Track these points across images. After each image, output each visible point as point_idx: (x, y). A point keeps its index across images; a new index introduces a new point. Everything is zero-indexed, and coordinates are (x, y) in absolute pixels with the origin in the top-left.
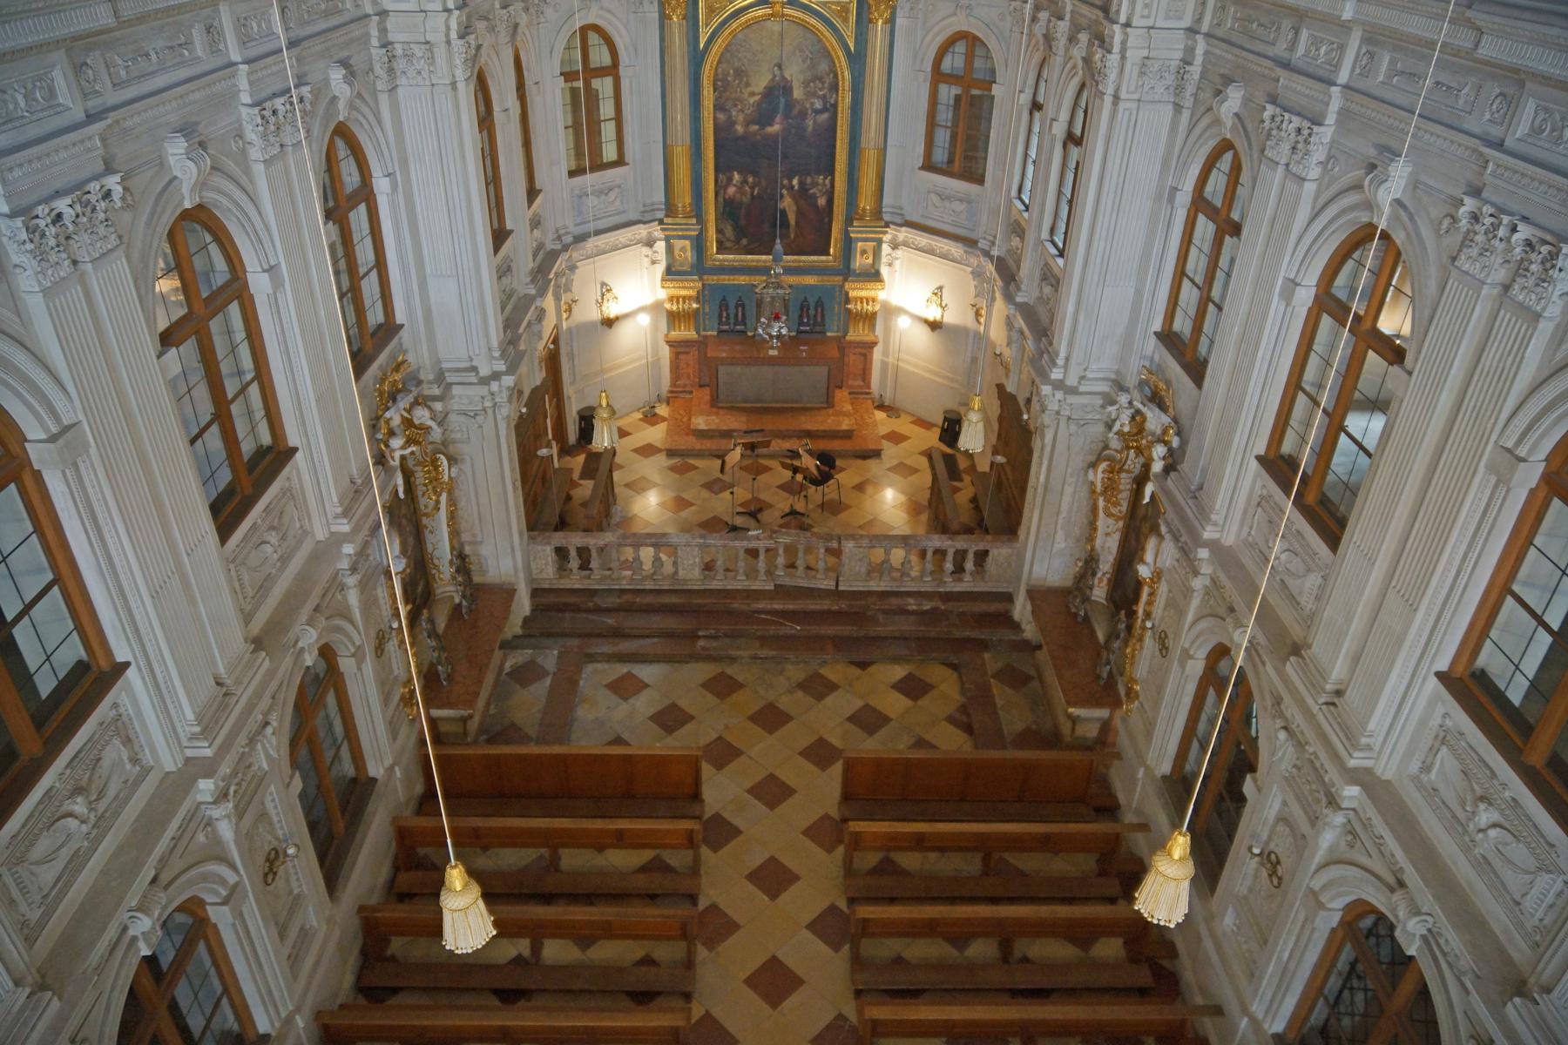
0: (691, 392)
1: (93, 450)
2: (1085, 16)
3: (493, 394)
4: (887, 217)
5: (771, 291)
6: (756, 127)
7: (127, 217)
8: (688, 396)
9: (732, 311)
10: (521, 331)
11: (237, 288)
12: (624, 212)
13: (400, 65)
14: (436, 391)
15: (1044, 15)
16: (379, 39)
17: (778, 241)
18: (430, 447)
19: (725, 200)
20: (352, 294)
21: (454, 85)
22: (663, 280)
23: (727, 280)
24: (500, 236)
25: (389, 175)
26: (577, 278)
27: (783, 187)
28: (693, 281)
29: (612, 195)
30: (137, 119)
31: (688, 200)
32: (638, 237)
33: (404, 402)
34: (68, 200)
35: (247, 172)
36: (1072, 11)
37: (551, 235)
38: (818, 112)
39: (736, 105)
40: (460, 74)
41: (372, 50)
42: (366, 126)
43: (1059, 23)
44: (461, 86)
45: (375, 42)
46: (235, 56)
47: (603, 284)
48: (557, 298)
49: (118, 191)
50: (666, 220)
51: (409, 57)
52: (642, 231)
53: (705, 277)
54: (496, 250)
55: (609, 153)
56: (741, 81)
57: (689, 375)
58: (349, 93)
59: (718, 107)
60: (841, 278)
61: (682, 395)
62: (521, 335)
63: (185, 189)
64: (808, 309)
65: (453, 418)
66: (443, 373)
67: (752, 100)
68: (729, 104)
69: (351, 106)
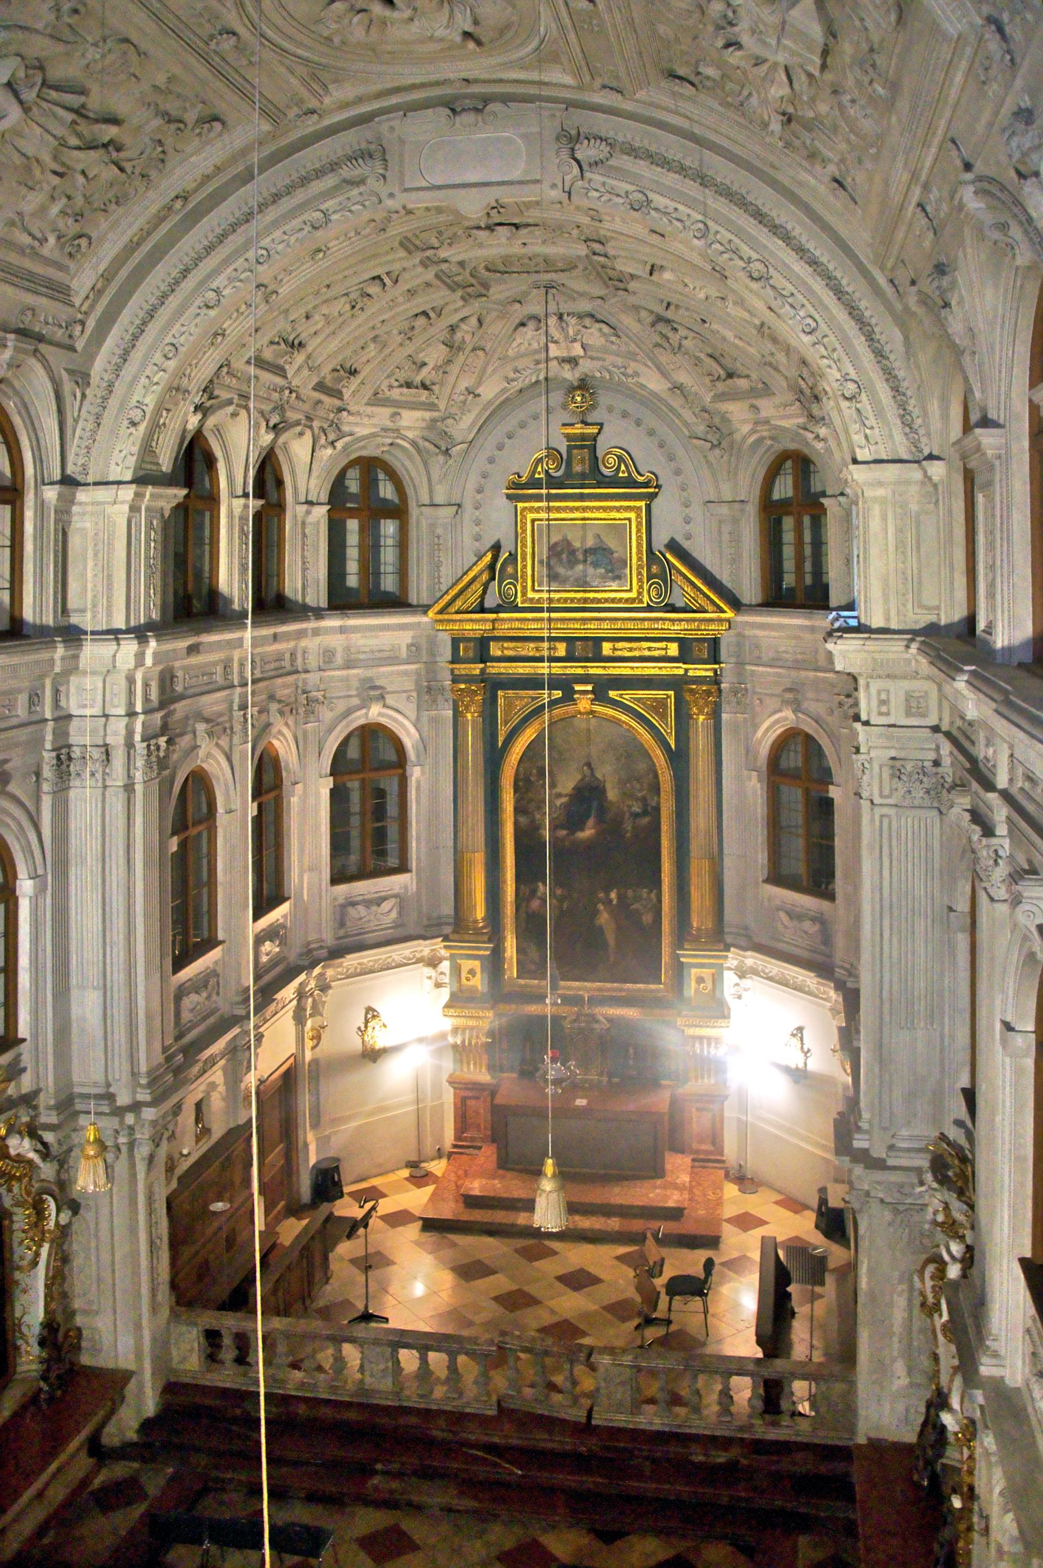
0: (480, 1148)
4: (729, 939)
6: (564, 832)
8: (476, 1152)
12: (402, 925)
16: (53, 742)
18: (37, 1185)
21: (129, 788)
27: (600, 901)
29: (386, 906)
32: (418, 955)
38: (636, 815)
40: (139, 776)
41: (45, 754)
44: (139, 788)
45: (48, 746)
47: (369, 1009)
52: (424, 948)
59: (518, 810)
61: (467, 1151)
68: (532, 806)
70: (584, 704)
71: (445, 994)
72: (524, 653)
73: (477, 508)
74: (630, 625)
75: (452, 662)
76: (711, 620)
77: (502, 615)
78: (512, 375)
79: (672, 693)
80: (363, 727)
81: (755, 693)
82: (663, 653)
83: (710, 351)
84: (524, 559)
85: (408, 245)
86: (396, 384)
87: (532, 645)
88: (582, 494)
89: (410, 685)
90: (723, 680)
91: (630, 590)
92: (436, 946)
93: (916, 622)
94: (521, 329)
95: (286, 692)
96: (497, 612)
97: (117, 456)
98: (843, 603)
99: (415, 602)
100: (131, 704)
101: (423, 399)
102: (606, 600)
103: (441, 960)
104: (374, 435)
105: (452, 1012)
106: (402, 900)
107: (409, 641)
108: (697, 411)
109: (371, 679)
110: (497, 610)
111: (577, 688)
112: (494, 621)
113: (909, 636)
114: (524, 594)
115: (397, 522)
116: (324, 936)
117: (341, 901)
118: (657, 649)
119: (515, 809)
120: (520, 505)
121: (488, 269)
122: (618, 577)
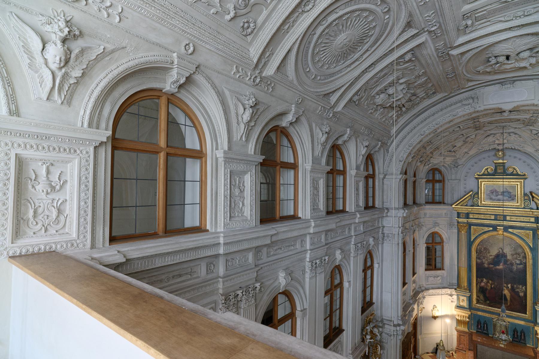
1: (307, 316)
3: (397, 331)
5: (500, 322)
6: (493, 266)
7: (326, 265)
9: (482, 325)
10: (407, 313)
11: (341, 285)
13: (386, 238)
14: (381, 325)
17: (503, 305)
19: (480, 286)
20: (364, 291)
21: (398, 244)
22: (455, 308)
23: (480, 313)
24: (404, 284)
25: (378, 263)
26: (425, 300)
28: (467, 311)
29: (439, 278)
30: (333, 245)
31: (466, 284)
32: (447, 293)
33: (372, 325)
34: (319, 260)
35: (349, 259)
37: (418, 287)
38: (518, 264)
39: (484, 258)
42: (375, 251)
45: (380, 233)
46: (353, 234)
48: (418, 306)
49: (327, 260)
50: (457, 289)
51: (388, 237)
52: (449, 291)
53: (472, 311)
54: (403, 287)
55: (439, 265)
56: (486, 252)
57: (464, 344)
58: (373, 244)
60: (533, 324)
62: (407, 315)
63: (338, 261)
64: (517, 332)
65: (383, 334)
66: (383, 320)
67: (491, 257)
68: (482, 258)
69: (373, 246)
70: (501, 232)
71: (455, 304)
72: (480, 217)
73: (465, 181)
80: (433, 232)
82: (529, 220)
87: (483, 215)
88: (487, 178)
91: (517, 203)
92: (453, 292)
99: (447, 203)
100: (399, 225)
101: (453, 154)
102: (509, 205)
103: (453, 295)
104: (439, 163)
105: (458, 310)
106: (443, 278)
107: (445, 212)
109: (436, 221)
111: (498, 228)
116: (423, 284)
117: (427, 275)
119: (476, 258)
120: (480, 180)
122: (513, 200)
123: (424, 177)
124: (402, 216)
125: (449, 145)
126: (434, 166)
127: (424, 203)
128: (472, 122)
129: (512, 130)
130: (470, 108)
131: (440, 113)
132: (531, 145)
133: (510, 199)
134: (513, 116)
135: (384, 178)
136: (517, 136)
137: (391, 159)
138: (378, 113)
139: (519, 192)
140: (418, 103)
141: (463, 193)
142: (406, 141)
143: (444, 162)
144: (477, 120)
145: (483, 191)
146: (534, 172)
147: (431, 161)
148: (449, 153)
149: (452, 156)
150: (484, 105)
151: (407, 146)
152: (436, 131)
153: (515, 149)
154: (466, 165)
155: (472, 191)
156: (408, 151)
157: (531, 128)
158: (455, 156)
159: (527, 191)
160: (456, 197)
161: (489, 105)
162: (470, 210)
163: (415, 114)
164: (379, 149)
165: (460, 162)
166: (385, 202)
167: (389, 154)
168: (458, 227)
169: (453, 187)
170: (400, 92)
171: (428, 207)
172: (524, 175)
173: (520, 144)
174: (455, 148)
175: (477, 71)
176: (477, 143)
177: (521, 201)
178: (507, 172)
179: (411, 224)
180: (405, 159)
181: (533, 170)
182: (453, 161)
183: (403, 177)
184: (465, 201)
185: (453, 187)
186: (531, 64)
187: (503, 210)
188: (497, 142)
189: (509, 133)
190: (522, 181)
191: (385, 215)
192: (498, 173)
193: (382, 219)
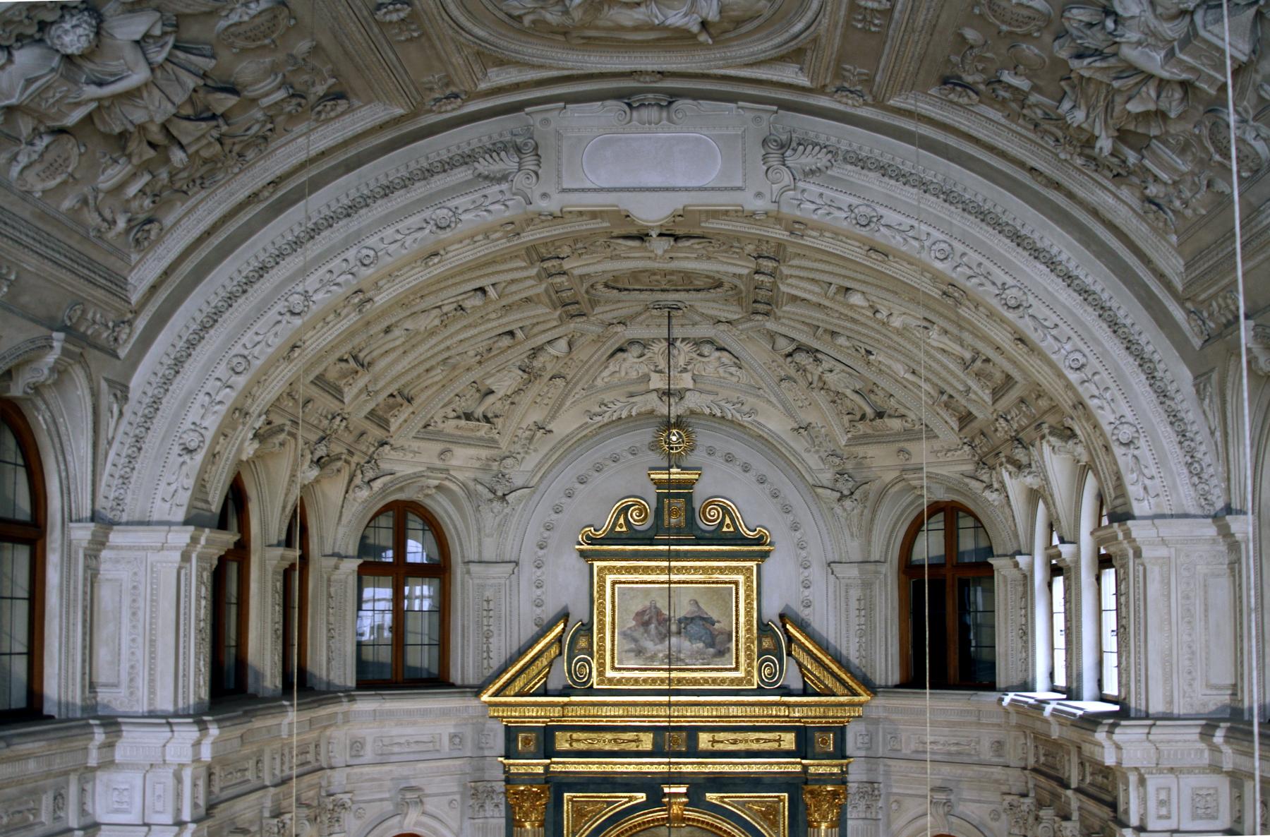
2: (1095, 815)
15: (1046, 813)
36: (1080, 808)
43: (1065, 824)
72: (597, 746)
74: (733, 711)
75: (507, 757)
76: (841, 705)
77: (573, 699)
78: (597, 409)
79: (786, 795)
81: (889, 794)
82: (775, 745)
83: (858, 387)
84: (602, 630)
85: (534, 254)
86: (453, 414)
87: (609, 736)
89: (454, 787)
90: (850, 778)
91: (736, 669)
93: (1204, 705)
94: (620, 355)
95: (311, 793)
96: (568, 695)
97: (163, 490)
98: (1016, 681)
99: (459, 682)
100: (178, 811)
101: (482, 433)
102: (706, 681)
104: (420, 475)
107: (452, 731)
108: (824, 455)
109: (406, 778)
110: (567, 691)
112: (564, 705)
113: (1111, 721)
114: (601, 673)
115: (436, 582)
118: (764, 741)
120: (597, 564)
121: (606, 286)
122: (721, 653)
123: (352, 548)
124: (187, 757)
125: (459, 386)
126: (401, 489)
127: (351, 682)
128: (533, 272)
129: (705, 331)
130: (508, 195)
131: (380, 208)
132: (779, 405)
133: (711, 650)
134: (690, 261)
135: (99, 543)
136: (726, 357)
137: (138, 439)
138: (23, 160)
139: (742, 619)
140: (256, 136)
141: (530, 630)
142: (215, 337)
143: (447, 470)
144: (556, 262)
145: (608, 619)
146: (795, 528)
147: (385, 466)
148: (463, 422)
149: (481, 439)
150: (564, 191)
151: (222, 371)
152: (370, 300)
153: (723, 417)
154: (542, 487)
155: (565, 616)
156: (229, 396)
157: (771, 325)
158: (493, 441)
159: (772, 611)
160: (500, 649)
161: (583, 190)
162: (557, 712)
163: (254, 197)
164: (60, 371)
165: (519, 473)
166: (106, 685)
167: (125, 408)
168: (507, 804)
169: (488, 601)
170: (131, 55)
171: (367, 705)
172: (759, 541)
173: (743, 398)
174: (491, 399)
175: (510, 16)
176: (579, 388)
177: (749, 657)
178: (702, 526)
179: (268, 803)
180: (215, 441)
181: (790, 517)
182: (486, 469)
183: (203, 541)
184: (534, 670)
185: (488, 601)
186: (704, 25)
187: (669, 704)
188: (657, 382)
189: (698, 343)
190: (753, 564)
191: (92, 762)
192: (669, 530)
193: (82, 781)
